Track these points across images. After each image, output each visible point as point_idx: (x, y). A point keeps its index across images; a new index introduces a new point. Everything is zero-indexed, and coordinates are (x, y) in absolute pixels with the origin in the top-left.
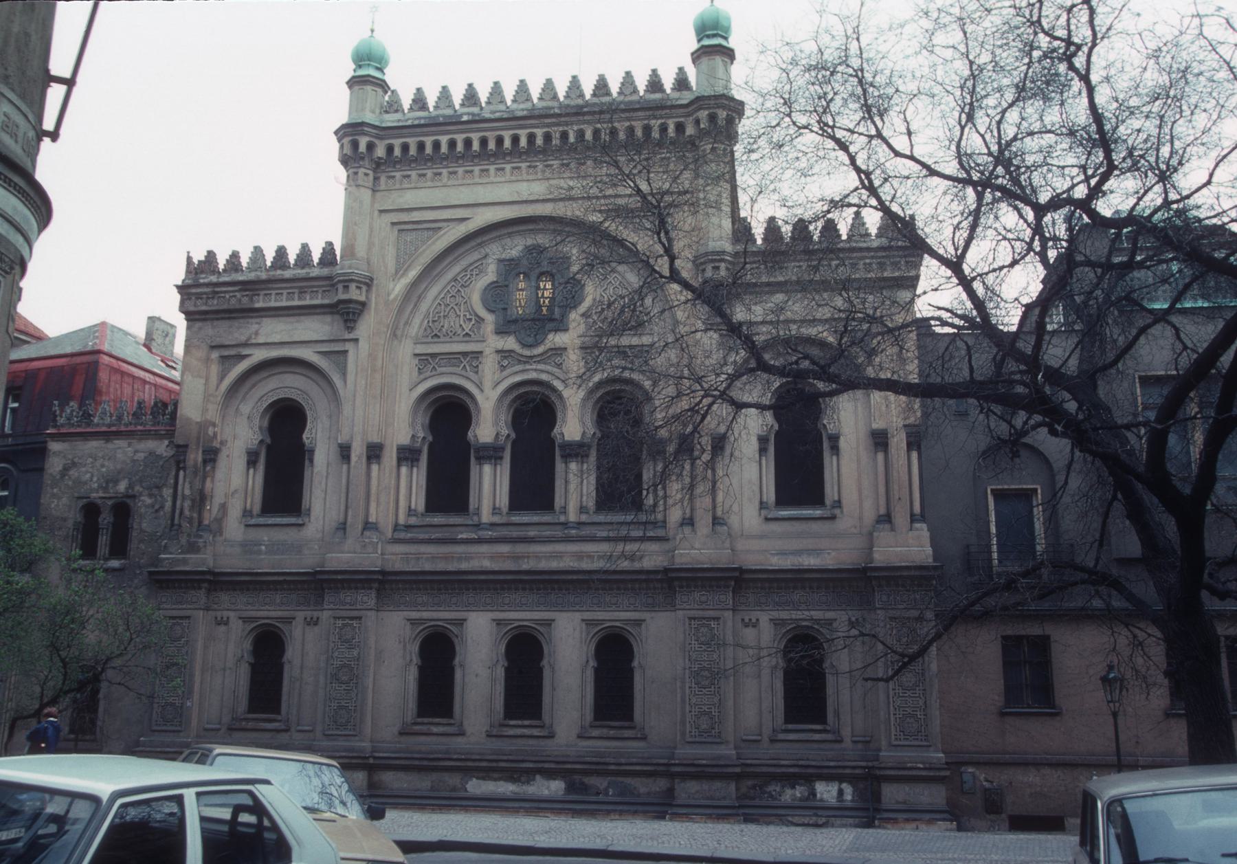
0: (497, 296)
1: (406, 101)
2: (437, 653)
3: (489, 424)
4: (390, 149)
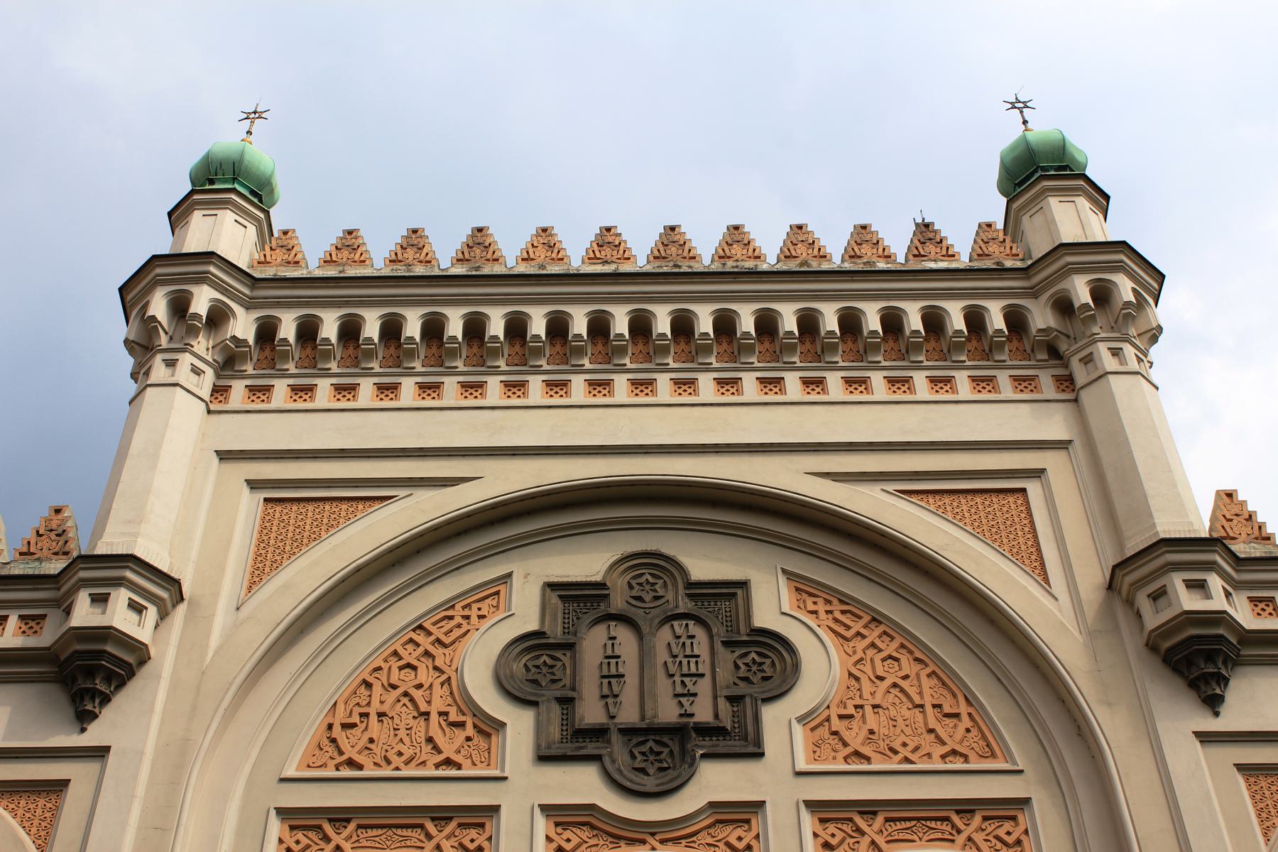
0: (538, 668)
4: (267, 332)
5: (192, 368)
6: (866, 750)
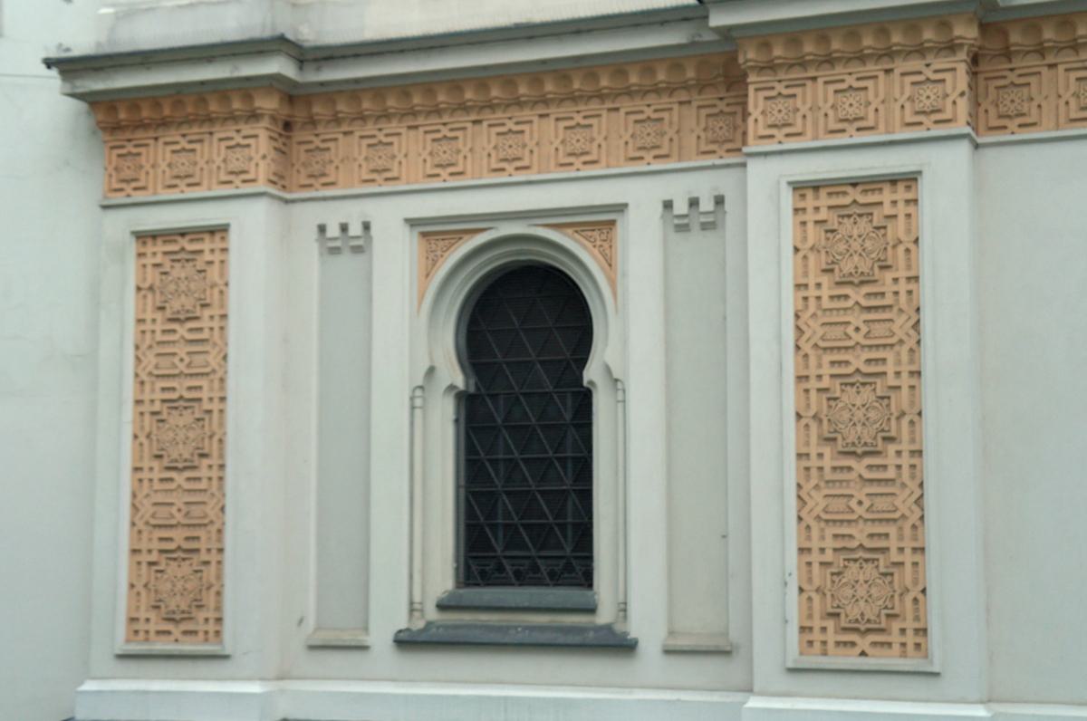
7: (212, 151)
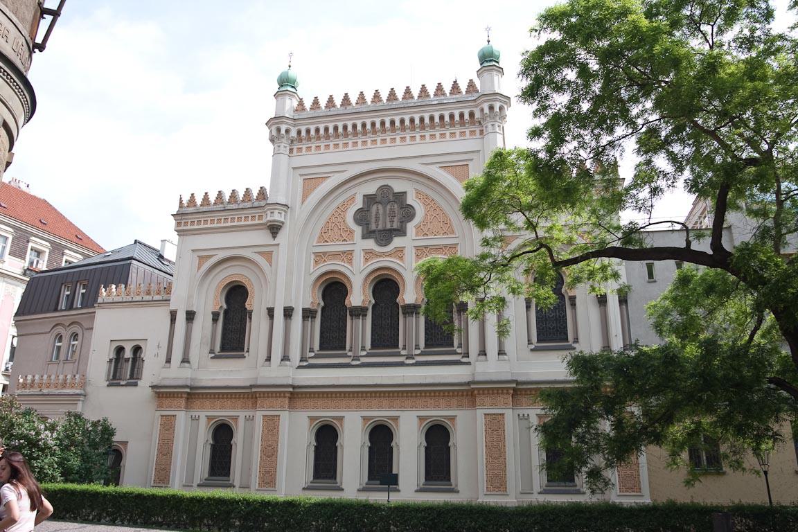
1: (308, 104)
2: (327, 437)
3: (358, 296)
4: (299, 132)
5: (284, 145)
6: (427, 233)
7: (175, 402)
